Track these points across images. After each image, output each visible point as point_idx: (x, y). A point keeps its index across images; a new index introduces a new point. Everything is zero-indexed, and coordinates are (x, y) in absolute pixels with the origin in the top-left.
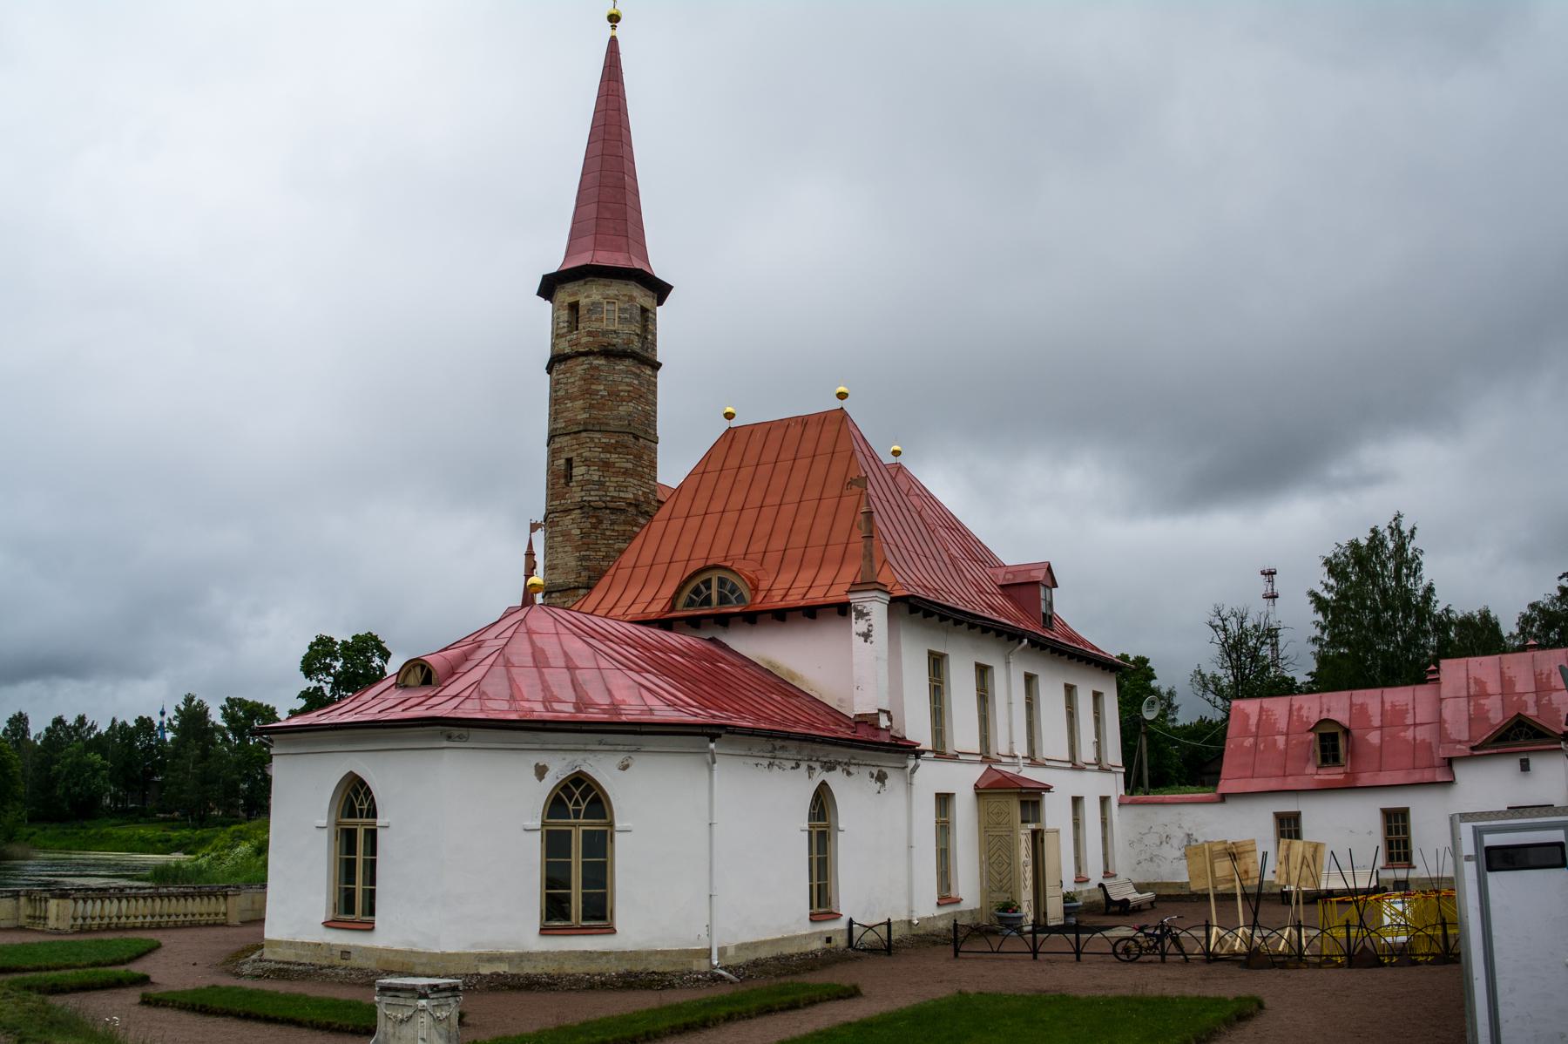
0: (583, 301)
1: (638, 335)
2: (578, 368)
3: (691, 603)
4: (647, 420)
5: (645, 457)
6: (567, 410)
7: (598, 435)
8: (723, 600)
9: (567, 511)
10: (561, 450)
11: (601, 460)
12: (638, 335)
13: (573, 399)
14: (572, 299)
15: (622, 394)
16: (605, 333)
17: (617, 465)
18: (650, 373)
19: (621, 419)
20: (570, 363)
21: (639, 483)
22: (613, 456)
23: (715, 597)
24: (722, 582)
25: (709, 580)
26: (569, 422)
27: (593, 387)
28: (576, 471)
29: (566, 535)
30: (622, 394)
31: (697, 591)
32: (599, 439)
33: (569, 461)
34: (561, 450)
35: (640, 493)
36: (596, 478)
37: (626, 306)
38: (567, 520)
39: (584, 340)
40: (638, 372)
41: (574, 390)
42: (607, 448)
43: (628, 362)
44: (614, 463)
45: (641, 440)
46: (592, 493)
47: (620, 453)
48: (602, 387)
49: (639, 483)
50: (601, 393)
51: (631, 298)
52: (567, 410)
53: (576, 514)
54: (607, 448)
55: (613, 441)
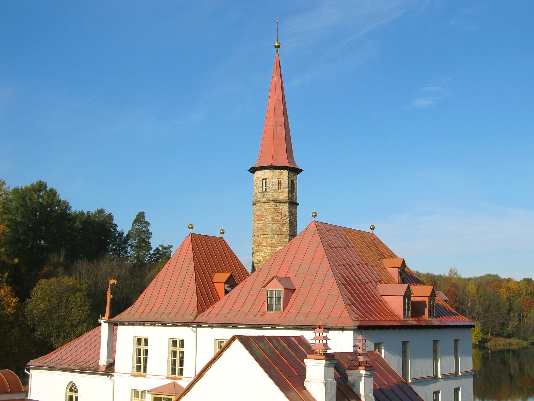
1: (260, 192)
4: (266, 226)
5: (264, 242)
18: (268, 205)
21: (261, 254)
35: (261, 258)
45: (262, 236)
49: (261, 254)
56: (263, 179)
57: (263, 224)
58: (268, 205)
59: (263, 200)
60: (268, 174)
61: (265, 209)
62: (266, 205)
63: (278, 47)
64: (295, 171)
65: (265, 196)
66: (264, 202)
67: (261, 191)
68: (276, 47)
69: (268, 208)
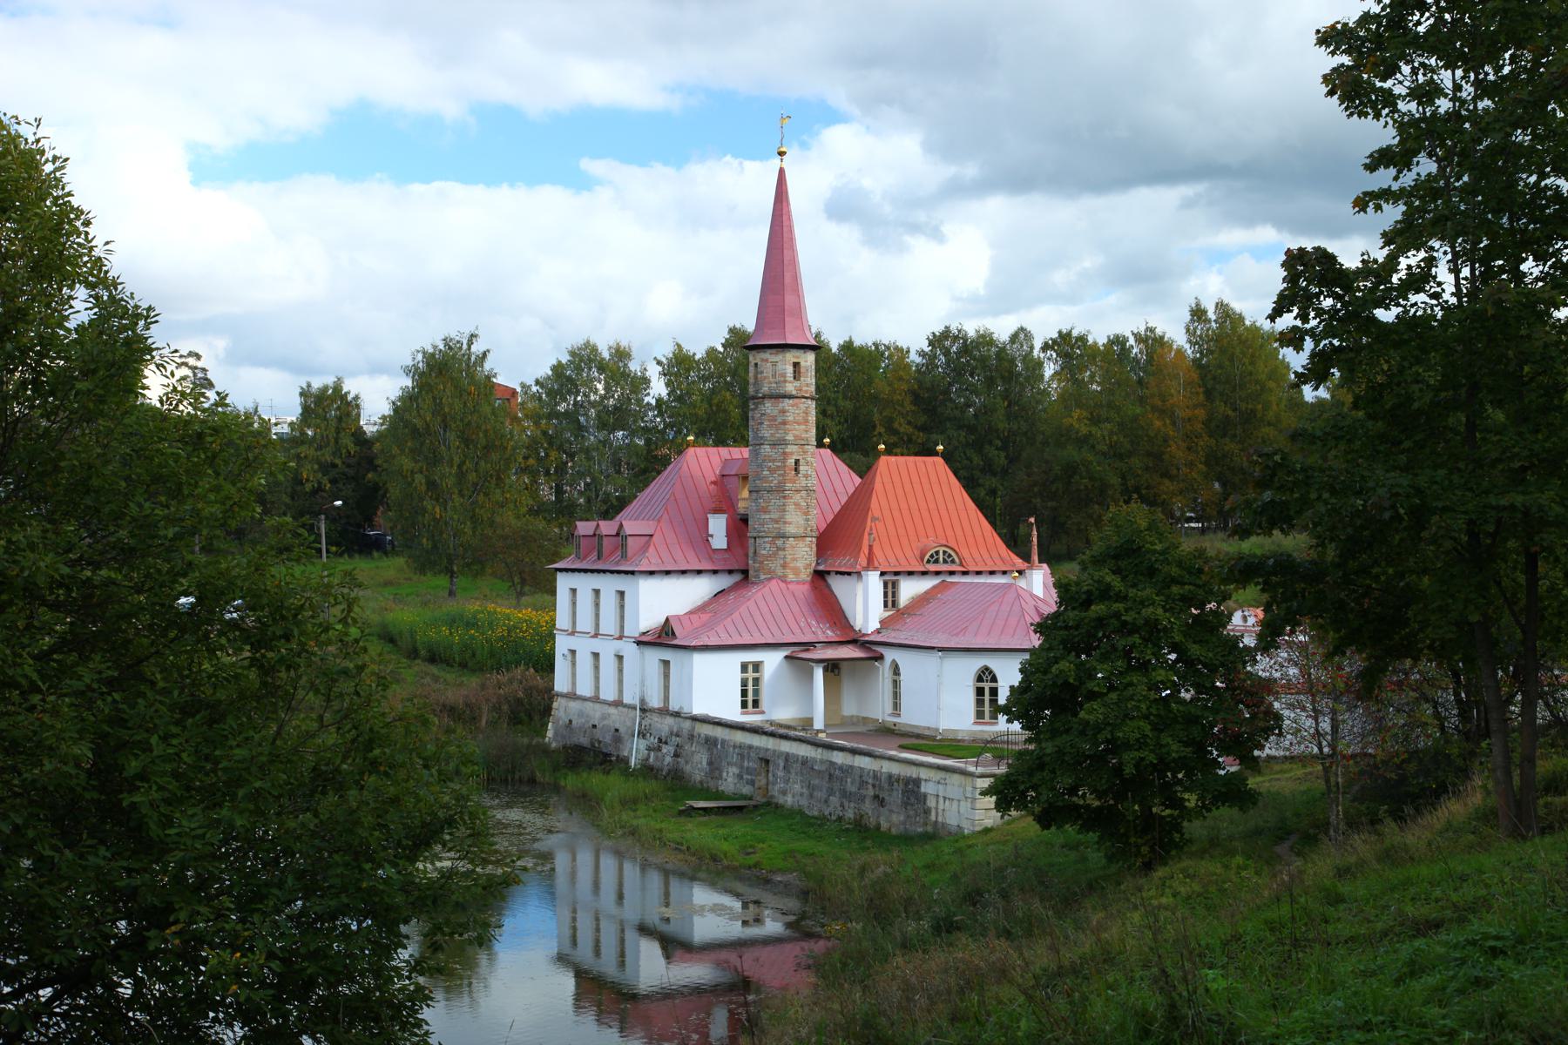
0: (802, 364)
2: (801, 405)
3: (928, 561)
6: (795, 429)
8: (945, 561)
9: (798, 491)
10: (792, 453)
13: (799, 424)
14: (796, 361)
20: (796, 400)
23: (941, 560)
24: (944, 552)
25: (937, 553)
26: (796, 437)
28: (801, 468)
29: (796, 504)
31: (932, 556)
33: (797, 462)
34: (792, 453)
38: (797, 497)
39: (805, 388)
41: (800, 419)
52: (795, 429)
53: (804, 493)
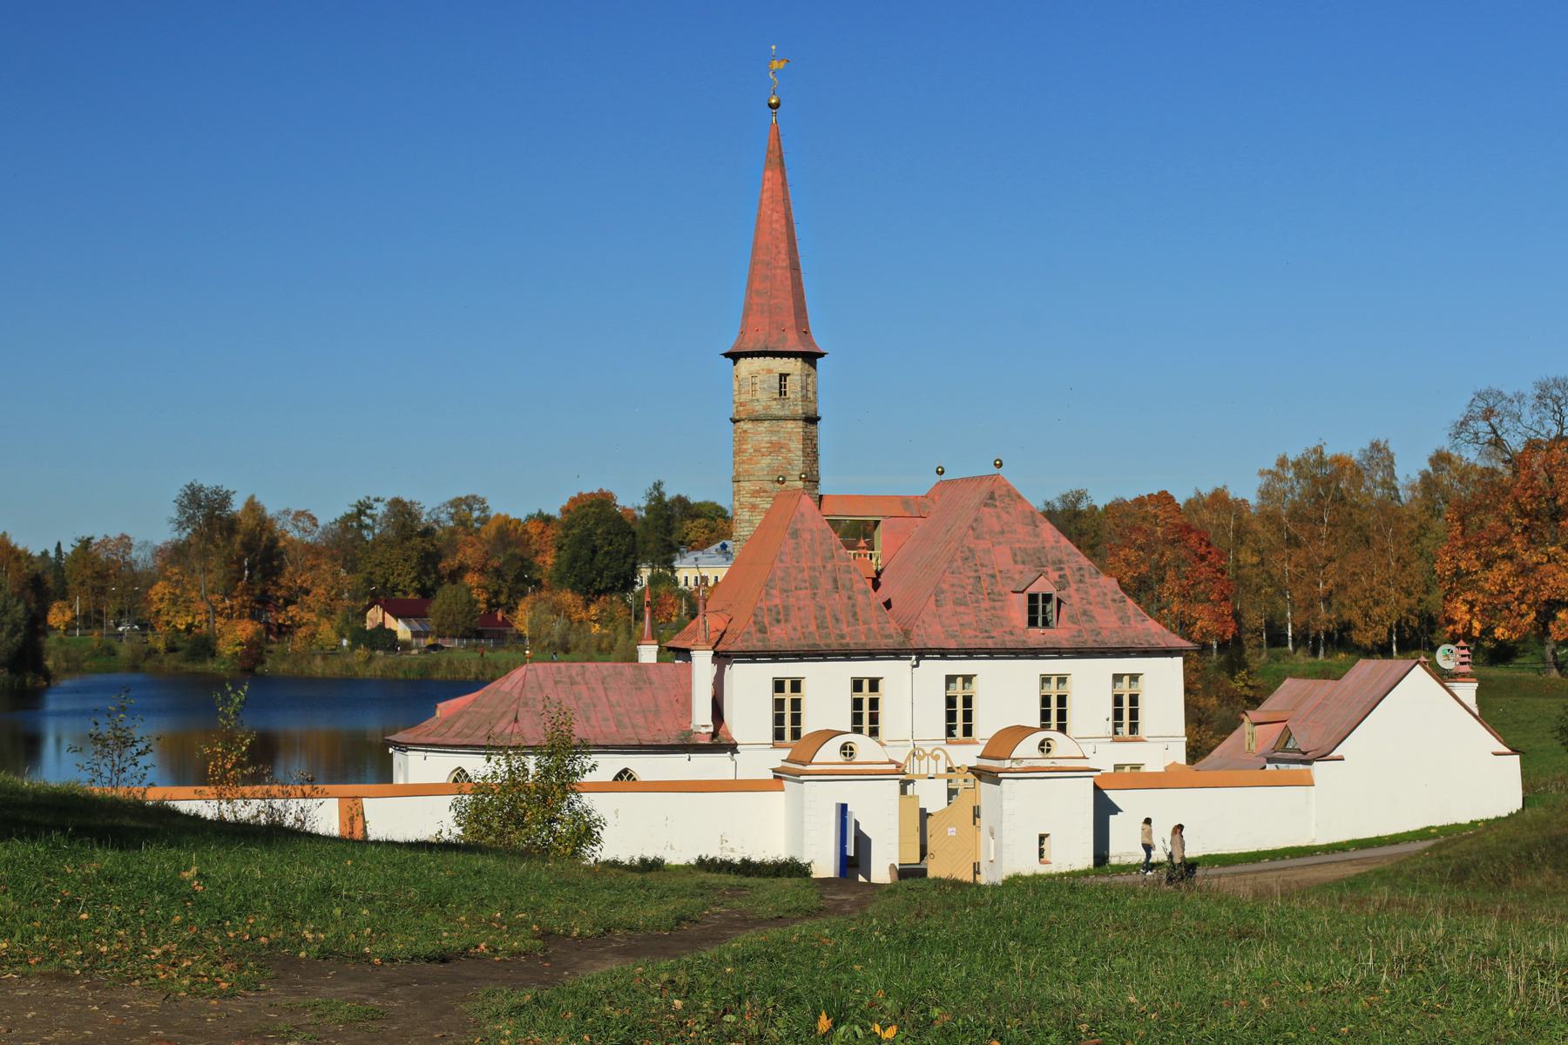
1: (775, 399)
4: (790, 464)
7: (747, 484)
11: (750, 503)
12: (775, 399)
15: (763, 450)
16: (752, 400)
17: (761, 506)
18: (793, 426)
19: (762, 469)
22: (758, 499)
27: (744, 447)
30: (763, 450)
32: (748, 487)
36: (747, 518)
37: (762, 379)
40: (777, 429)
42: (755, 494)
43: (766, 424)
44: (758, 504)
46: (746, 529)
47: (763, 497)
48: (749, 446)
50: (749, 451)
51: (770, 371)
54: (755, 494)
55: (758, 488)
56: (781, 375)
57: (785, 461)
58: (793, 426)
59: (781, 413)
60: (792, 366)
61: (787, 433)
62: (790, 425)
63: (776, 106)
64: (811, 358)
65: (786, 407)
66: (786, 419)
67: (778, 397)
68: (771, 106)
69: (794, 430)
